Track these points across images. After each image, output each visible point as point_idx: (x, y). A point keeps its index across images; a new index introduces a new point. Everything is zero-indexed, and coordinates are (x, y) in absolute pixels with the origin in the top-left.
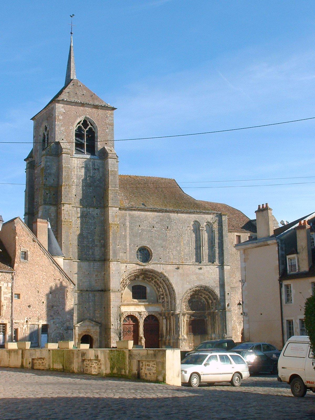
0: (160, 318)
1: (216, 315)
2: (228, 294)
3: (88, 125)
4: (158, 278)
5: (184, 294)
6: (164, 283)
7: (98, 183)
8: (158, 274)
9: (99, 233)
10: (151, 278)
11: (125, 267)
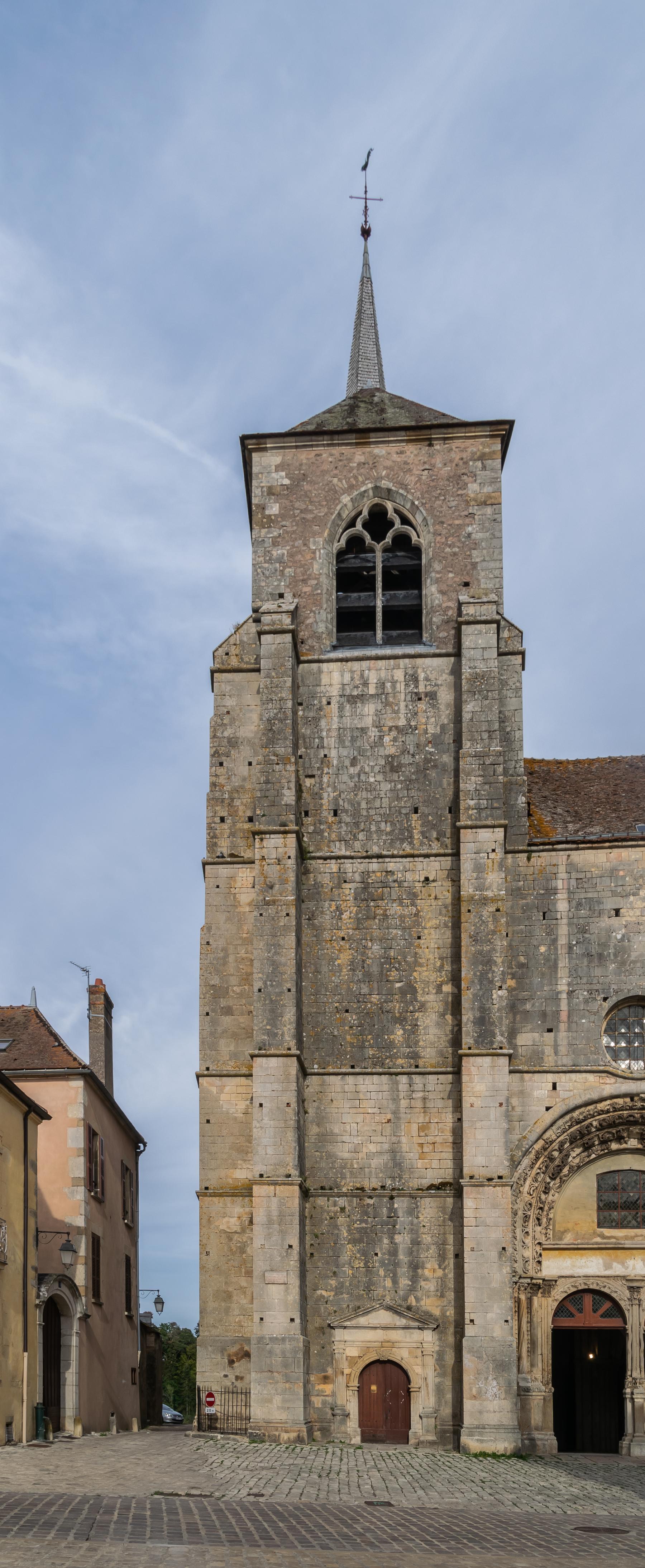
3: (392, 524)
7: (430, 753)
9: (437, 956)
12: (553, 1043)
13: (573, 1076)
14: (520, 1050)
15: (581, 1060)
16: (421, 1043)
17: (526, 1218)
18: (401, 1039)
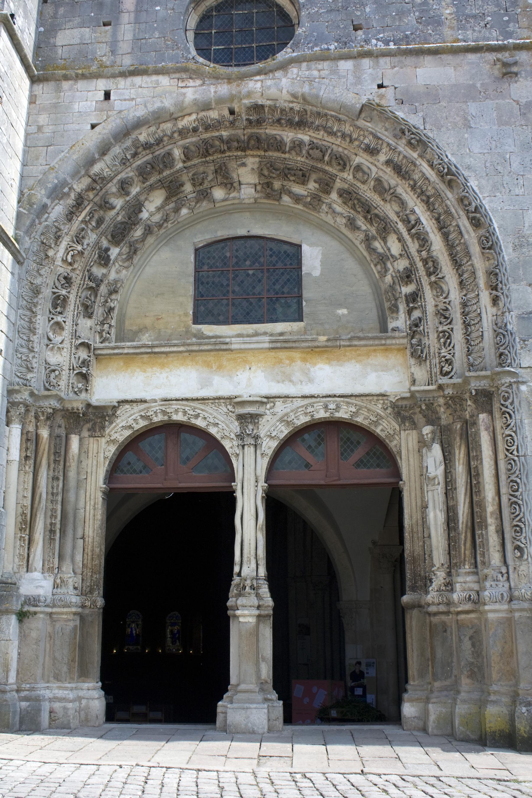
8: (347, 129)
10: (314, 169)
11: (102, 97)
13: (138, 80)
14: (60, 51)
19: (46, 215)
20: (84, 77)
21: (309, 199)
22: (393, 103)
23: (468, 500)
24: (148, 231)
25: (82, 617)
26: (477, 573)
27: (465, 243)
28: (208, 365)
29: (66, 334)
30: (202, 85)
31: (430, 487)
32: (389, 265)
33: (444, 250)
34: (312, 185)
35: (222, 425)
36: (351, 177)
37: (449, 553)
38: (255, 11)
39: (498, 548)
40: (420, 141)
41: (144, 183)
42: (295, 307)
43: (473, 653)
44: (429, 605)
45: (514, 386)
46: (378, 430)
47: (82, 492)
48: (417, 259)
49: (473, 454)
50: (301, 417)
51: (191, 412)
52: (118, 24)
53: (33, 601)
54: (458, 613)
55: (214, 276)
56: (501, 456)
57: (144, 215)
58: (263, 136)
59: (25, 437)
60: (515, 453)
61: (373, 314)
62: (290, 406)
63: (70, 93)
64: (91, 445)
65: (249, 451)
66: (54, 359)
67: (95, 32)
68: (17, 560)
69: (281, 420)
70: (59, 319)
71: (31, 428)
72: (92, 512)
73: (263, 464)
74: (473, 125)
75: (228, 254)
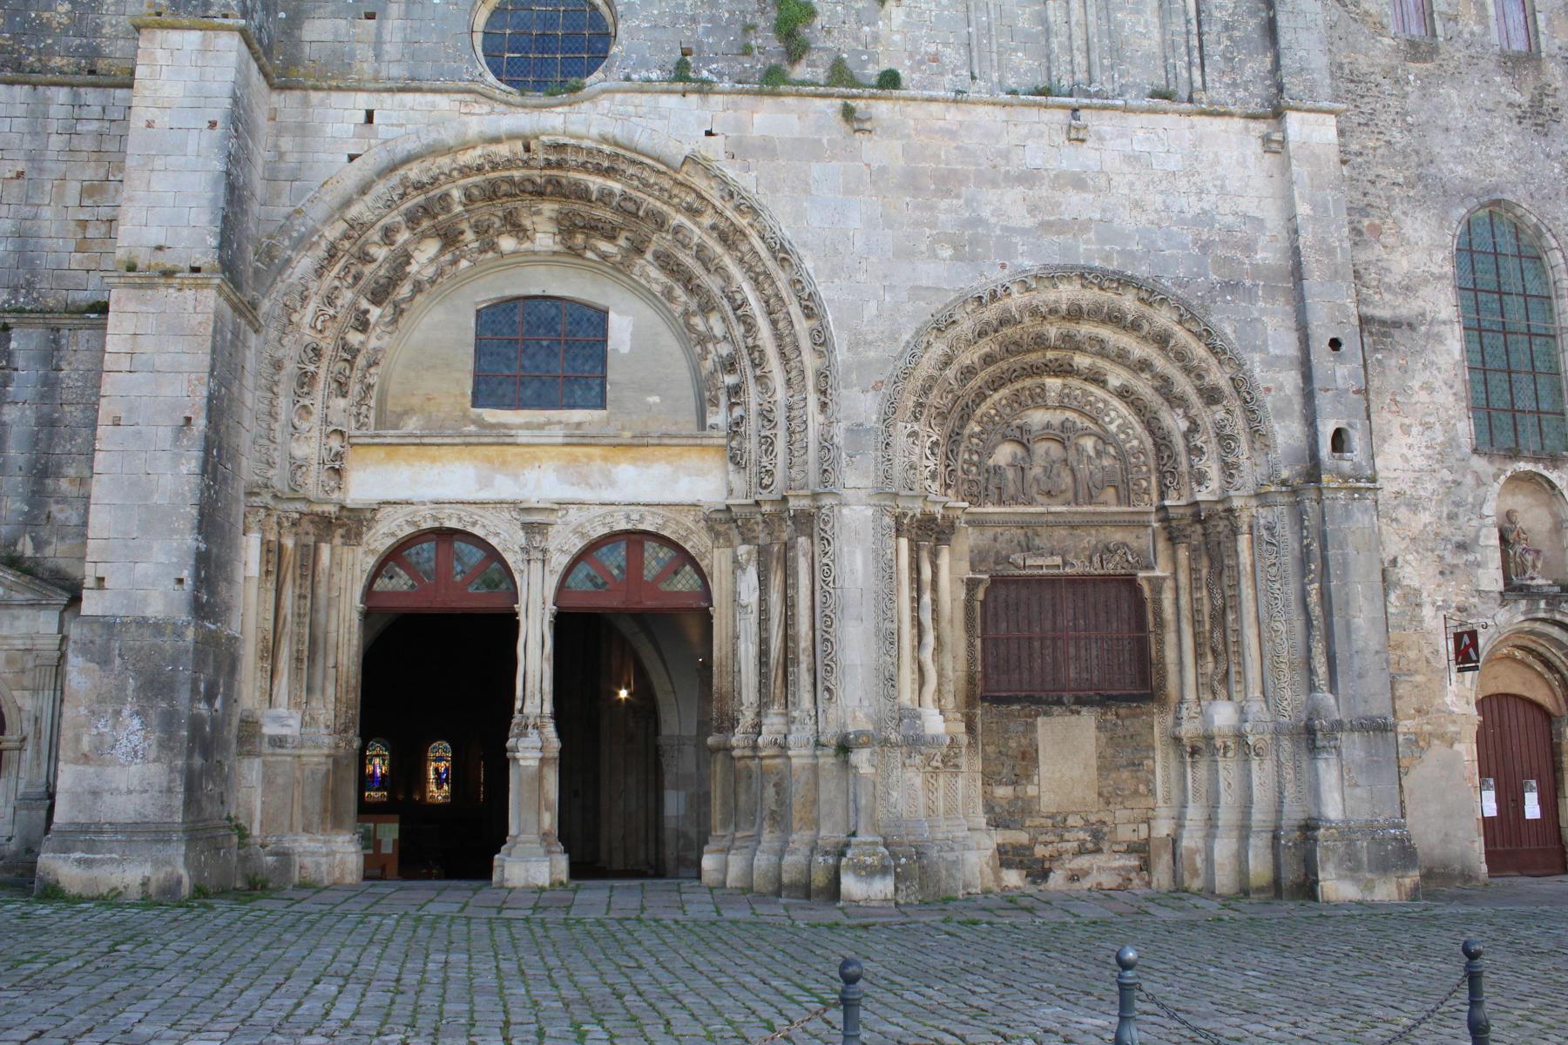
0: (718, 562)
1: (1235, 532)
2: (1335, 344)
4: (679, 219)
5: (906, 337)
6: (728, 262)
12: (373, 38)
13: (409, 98)
14: (307, 49)
15: (426, 70)
16: (106, 30)
17: (306, 380)
18: (65, 20)
19: (290, 270)
20: (338, 89)
21: (619, 258)
22: (722, 156)
23: (781, 634)
24: (418, 287)
25: (336, 762)
26: (787, 715)
27: (795, 336)
28: (489, 460)
29: (315, 419)
30: (489, 114)
31: (743, 616)
32: (710, 346)
33: (772, 338)
34: (622, 242)
35: (504, 535)
36: (669, 237)
37: (760, 691)
38: (562, 8)
39: (809, 687)
40: (751, 207)
41: (414, 229)
42: (597, 389)
43: (777, 801)
44: (733, 748)
45: (836, 509)
46: (687, 547)
47: (334, 613)
48: (742, 345)
49: (790, 581)
50: (598, 528)
51: (467, 519)
52: (385, 17)
53: (278, 742)
54: (761, 758)
55: (498, 346)
56: (817, 587)
57: (413, 268)
58: (564, 181)
59: (265, 547)
60: (831, 584)
61: (691, 404)
62: (587, 514)
63: (321, 110)
64: (345, 556)
65: (536, 567)
66: (301, 450)
67: (354, 27)
68: (257, 694)
69: (575, 532)
70: (307, 402)
71: (272, 537)
72: (347, 636)
73: (552, 582)
74: (814, 192)
75: (517, 319)
